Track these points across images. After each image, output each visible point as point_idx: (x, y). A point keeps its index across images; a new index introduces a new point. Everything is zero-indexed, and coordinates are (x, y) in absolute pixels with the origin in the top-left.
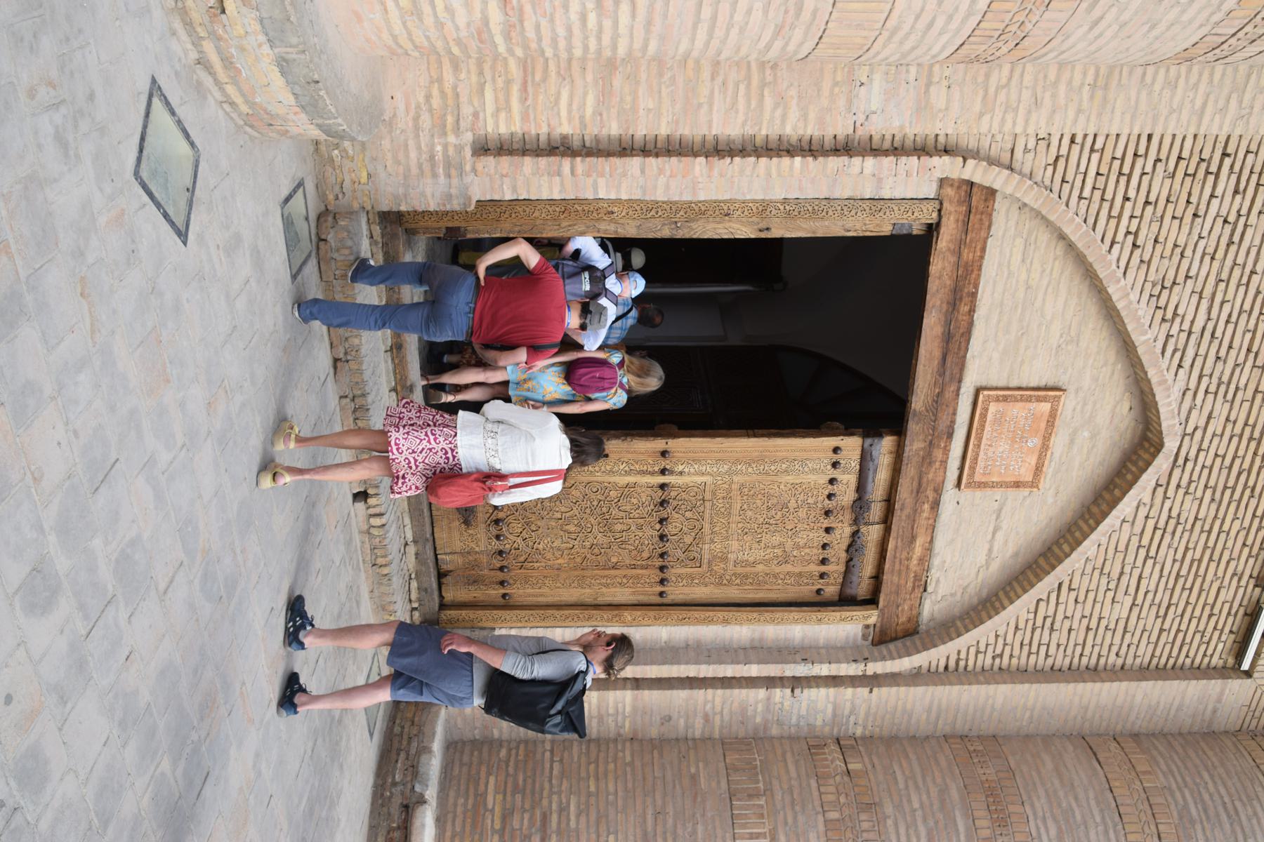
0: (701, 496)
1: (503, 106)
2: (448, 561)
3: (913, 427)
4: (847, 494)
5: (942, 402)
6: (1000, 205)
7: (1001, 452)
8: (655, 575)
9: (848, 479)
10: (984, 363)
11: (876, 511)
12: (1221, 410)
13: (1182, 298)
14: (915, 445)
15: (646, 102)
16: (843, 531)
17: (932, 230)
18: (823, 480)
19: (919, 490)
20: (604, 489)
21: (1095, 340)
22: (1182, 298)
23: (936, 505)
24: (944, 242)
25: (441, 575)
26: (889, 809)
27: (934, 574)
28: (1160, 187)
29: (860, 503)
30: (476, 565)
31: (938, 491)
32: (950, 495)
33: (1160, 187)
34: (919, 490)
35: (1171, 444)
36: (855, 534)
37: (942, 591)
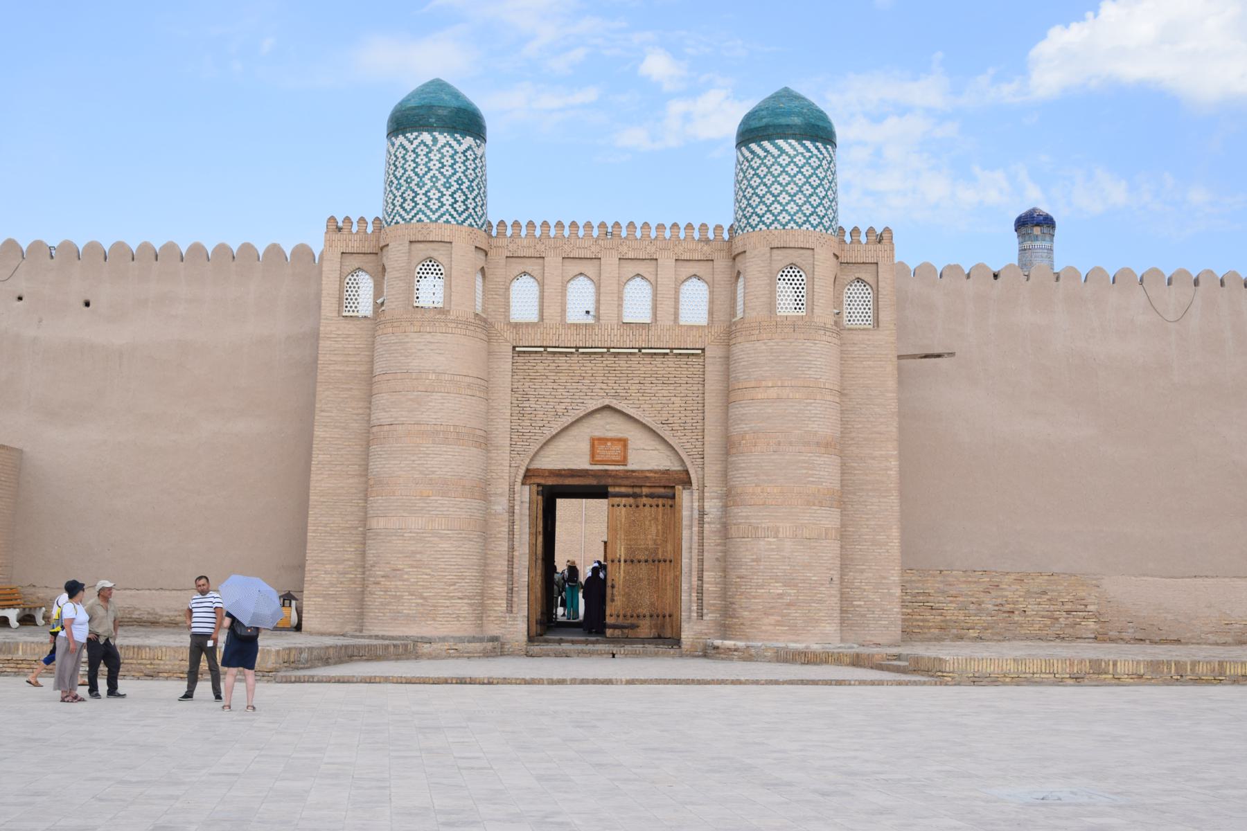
0: (629, 549)
1: (499, 605)
2: (653, 633)
3: (603, 482)
4: (631, 500)
5: (594, 474)
6: (532, 467)
7: (614, 452)
8: (662, 564)
9: (624, 501)
10: (583, 464)
11: (637, 490)
12: (599, 385)
13: (560, 408)
14: (610, 481)
15: (499, 568)
16: (644, 500)
17: (538, 485)
18: (624, 509)
19: (627, 478)
20: (625, 580)
21: (574, 431)
22: (560, 408)
23: (633, 471)
24: (542, 481)
25: (659, 637)
27: (661, 468)
28: (527, 423)
29: (635, 496)
30: (656, 626)
31: (627, 471)
32: (629, 467)
33: (527, 423)
34: (627, 478)
35: (607, 402)
36: (646, 496)
37: (669, 464)
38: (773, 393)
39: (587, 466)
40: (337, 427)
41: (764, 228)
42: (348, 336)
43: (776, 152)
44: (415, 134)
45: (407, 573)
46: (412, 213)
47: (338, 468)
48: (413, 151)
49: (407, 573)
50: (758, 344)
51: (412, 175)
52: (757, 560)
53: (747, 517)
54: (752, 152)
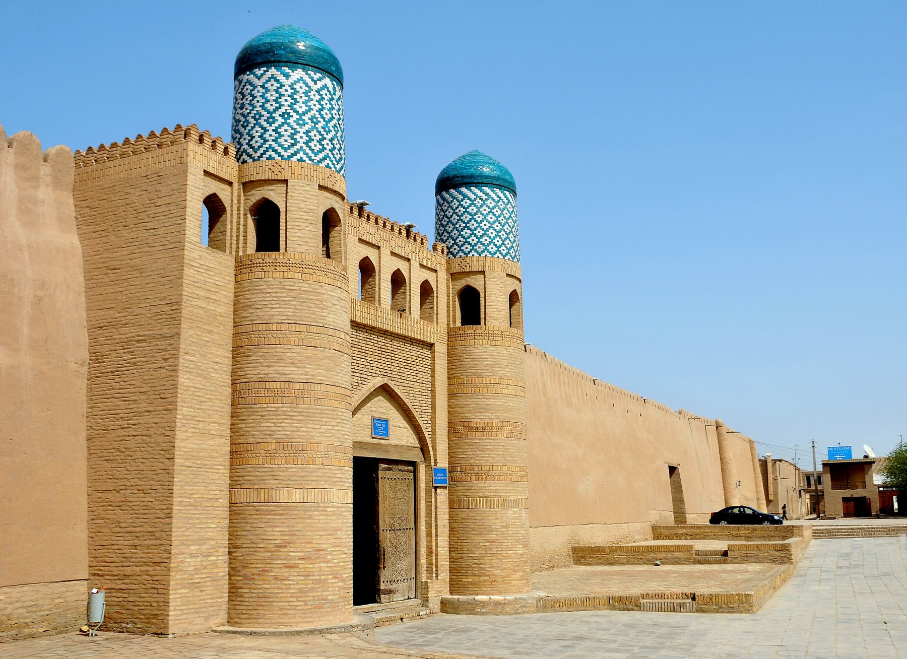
26: (472, 461)
35: (386, 380)
38: (512, 390)
39: (369, 439)
40: (200, 375)
41: (501, 257)
42: (209, 269)
43: (506, 201)
44: (319, 75)
45: (331, 553)
46: (321, 156)
47: (201, 425)
48: (318, 91)
49: (331, 553)
50: (501, 349)
51: (318, 116)
52: (507, 527)
53: (496, 491)
54: (486, 194)
